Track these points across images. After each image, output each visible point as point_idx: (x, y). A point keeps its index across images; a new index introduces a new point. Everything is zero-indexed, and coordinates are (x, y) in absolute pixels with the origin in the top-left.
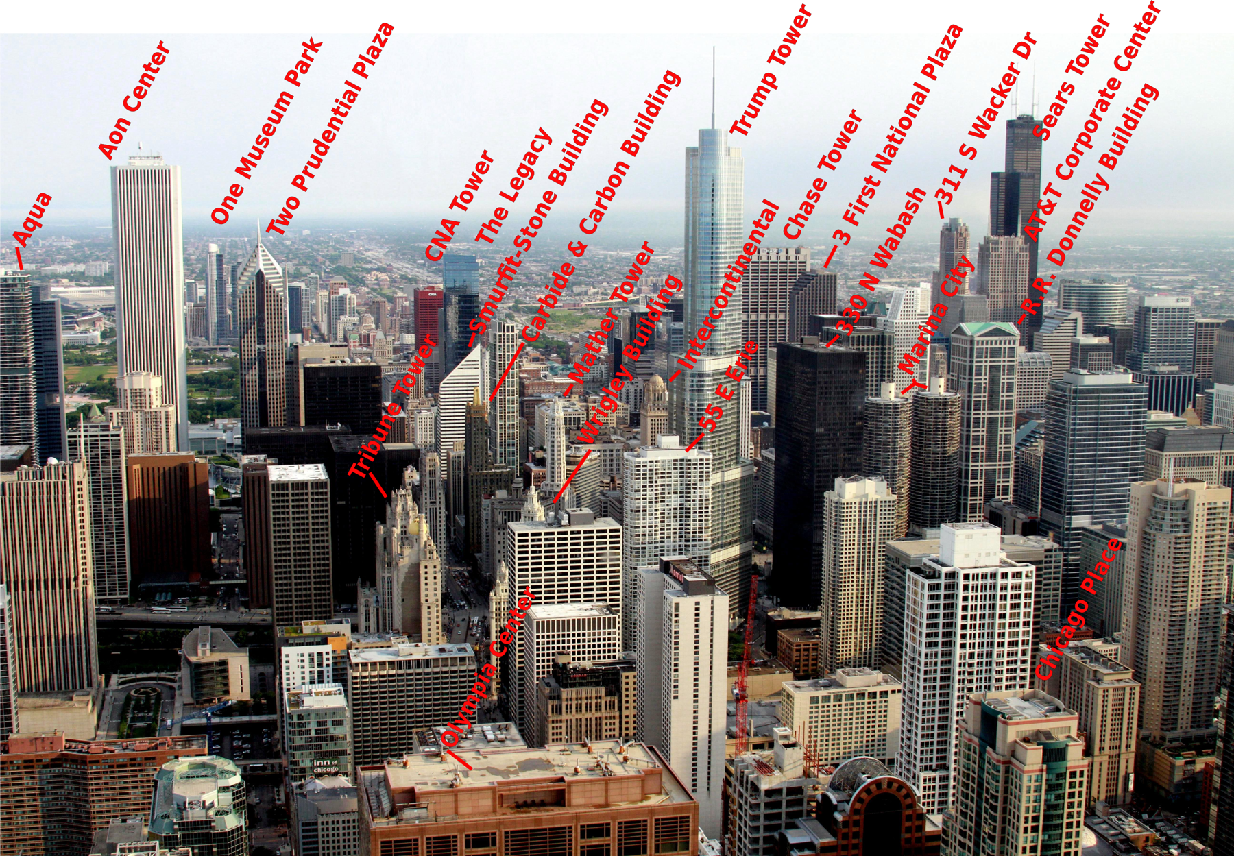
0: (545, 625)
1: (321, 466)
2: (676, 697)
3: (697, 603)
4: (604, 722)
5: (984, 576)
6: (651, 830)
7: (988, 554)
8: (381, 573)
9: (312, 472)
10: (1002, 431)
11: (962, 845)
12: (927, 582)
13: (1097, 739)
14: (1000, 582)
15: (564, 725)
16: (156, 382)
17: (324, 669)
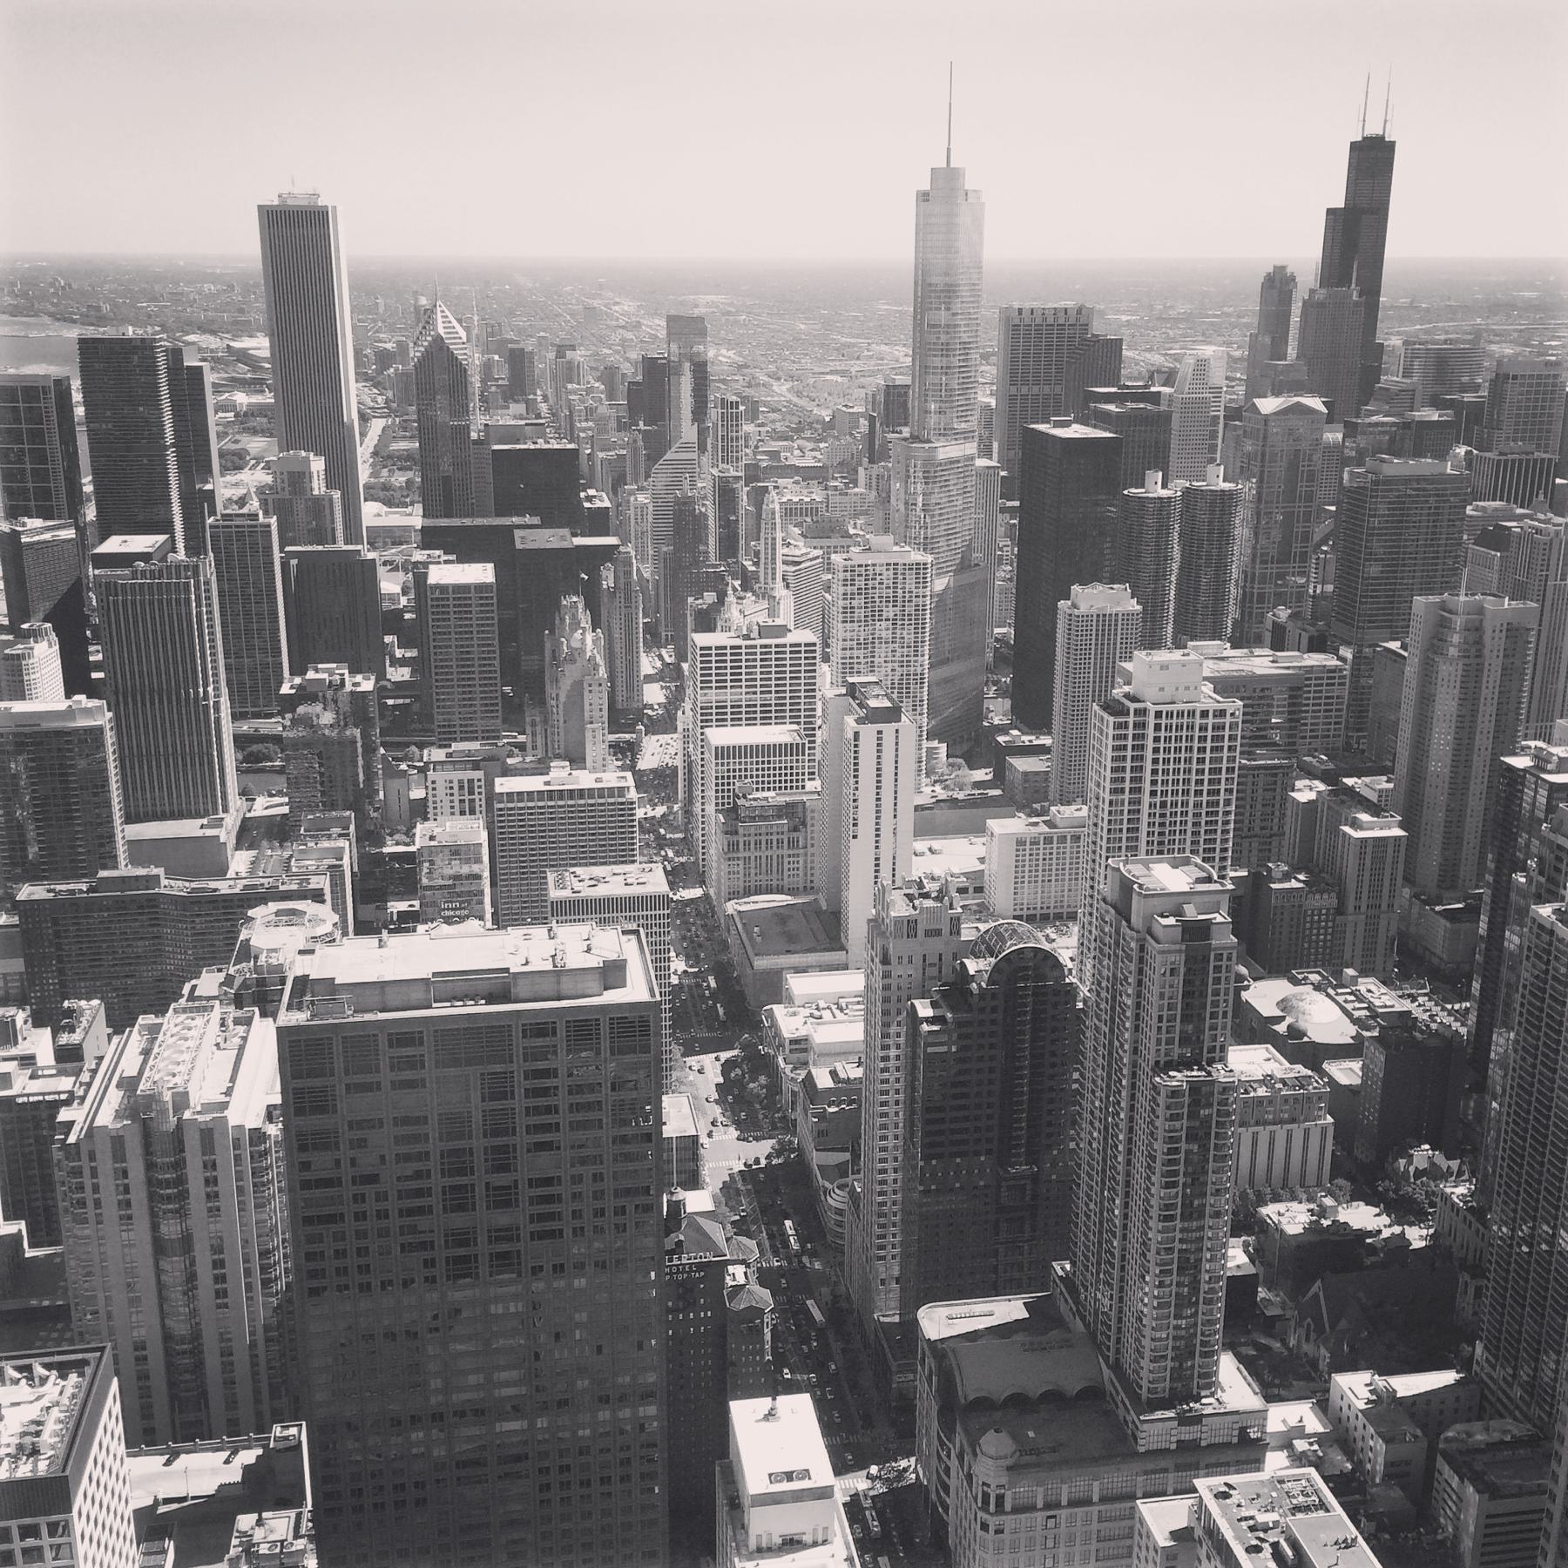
0: (722, 753)
1: (490, 566)
2: (855, 837)
3: (880, 732)
4: (786, 860)
5: (1180, 714)
6: (605, 1030)
7: (1187, 688)
8: (550, 690)
9: (481, 573)
10: (1299, 528)
11: (1097, 1029)
12: (1112, 719)
13: (1352, 896)
14: (1198, 721)
15: (741, 862)
16: (318, 465)
17: (476, 797)
